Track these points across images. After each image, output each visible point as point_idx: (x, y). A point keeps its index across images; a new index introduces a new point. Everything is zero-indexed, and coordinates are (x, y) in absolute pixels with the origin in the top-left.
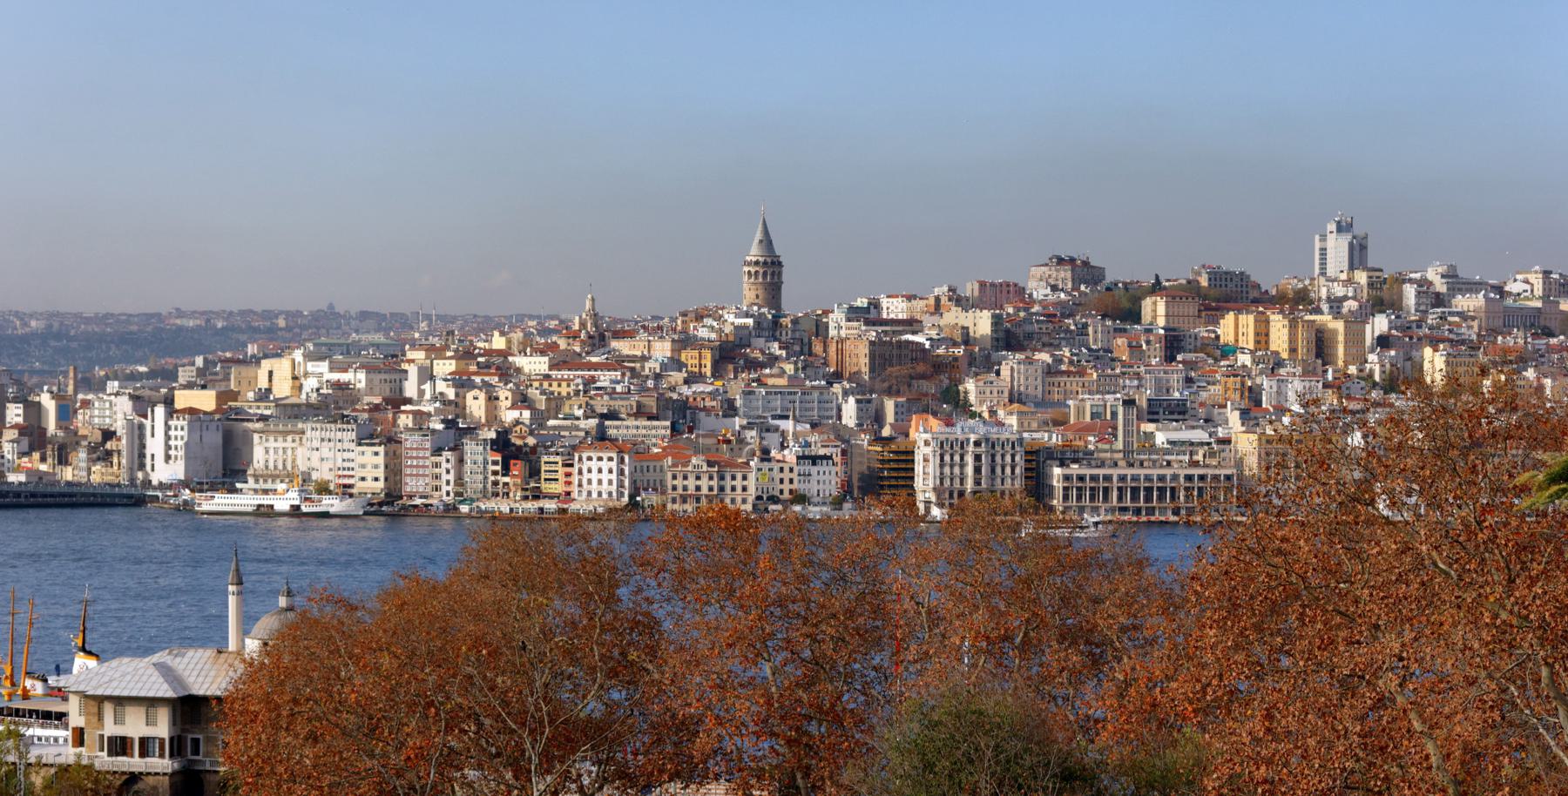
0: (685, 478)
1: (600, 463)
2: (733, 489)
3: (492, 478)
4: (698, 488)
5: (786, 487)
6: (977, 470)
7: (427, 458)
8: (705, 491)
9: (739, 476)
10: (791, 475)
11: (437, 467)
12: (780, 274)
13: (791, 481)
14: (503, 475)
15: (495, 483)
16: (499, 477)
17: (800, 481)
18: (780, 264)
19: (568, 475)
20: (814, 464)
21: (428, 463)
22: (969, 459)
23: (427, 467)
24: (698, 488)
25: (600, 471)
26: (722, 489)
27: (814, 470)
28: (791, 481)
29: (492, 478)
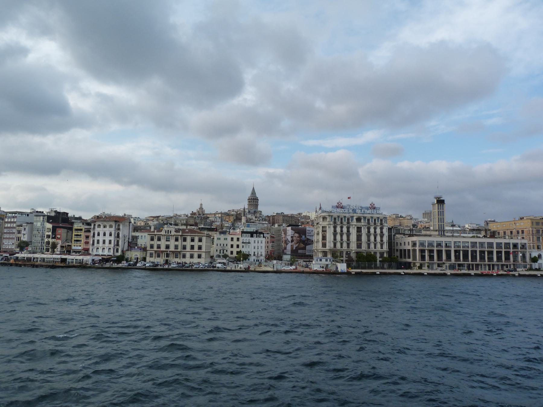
0: (159, 239)
1: (105, 229)
2: (192, 247)
3: (46, 240)
4: (168, 247)
5: (235, 250)
6: (359, 238)
7: (14, 228)
8: (172, 248)
9: (196, 239)
10: (238, 243)
11: (19, 233)
12: (258, 202)
13: (238, 246)
14: (53, 238)
15: (48, 243)
17: (243, 247)
18: (258, 200)
19: (87, 237)
20: (252, 236)
21: (14, 231)
22: (354, 232)
23: (14, 233)
24: (168, 247)
25: (105, 235)
26: (184, 247)
27: (252, 240)
28: (238, 246)
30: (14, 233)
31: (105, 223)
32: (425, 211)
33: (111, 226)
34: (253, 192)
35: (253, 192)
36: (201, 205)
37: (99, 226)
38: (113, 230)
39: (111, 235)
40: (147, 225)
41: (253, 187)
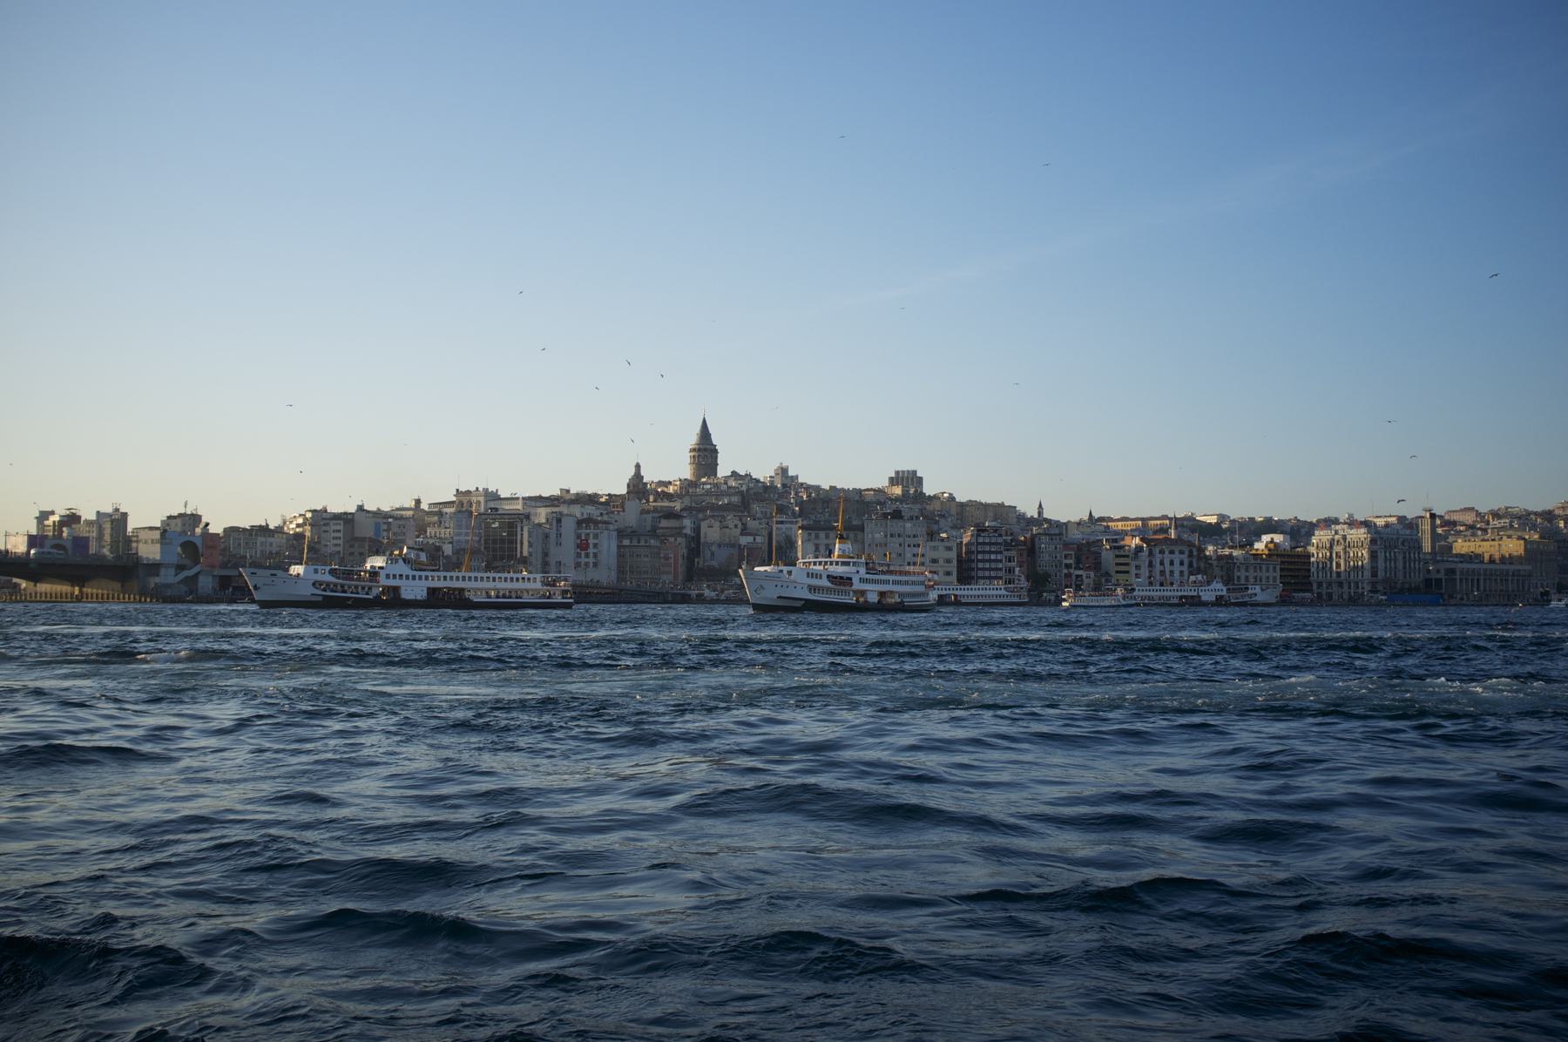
3: (1065, 571)
7: (1001, 553)
11: (1010, 561)
15: (1068, 576)
16: (1072, 571)
29: (1065, 571)
30: (1001, 561)
31: (1173, 548)
32: (897, 473)
33: (1181, 552)
34: (705, 433)
35: (705, 433)
36: (638, 467)
37: (1162, 552)
38: (1185, 557)
39: (1182, 563)
40: (440, 514)
41: (704, 421)
